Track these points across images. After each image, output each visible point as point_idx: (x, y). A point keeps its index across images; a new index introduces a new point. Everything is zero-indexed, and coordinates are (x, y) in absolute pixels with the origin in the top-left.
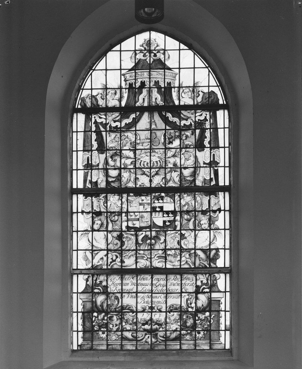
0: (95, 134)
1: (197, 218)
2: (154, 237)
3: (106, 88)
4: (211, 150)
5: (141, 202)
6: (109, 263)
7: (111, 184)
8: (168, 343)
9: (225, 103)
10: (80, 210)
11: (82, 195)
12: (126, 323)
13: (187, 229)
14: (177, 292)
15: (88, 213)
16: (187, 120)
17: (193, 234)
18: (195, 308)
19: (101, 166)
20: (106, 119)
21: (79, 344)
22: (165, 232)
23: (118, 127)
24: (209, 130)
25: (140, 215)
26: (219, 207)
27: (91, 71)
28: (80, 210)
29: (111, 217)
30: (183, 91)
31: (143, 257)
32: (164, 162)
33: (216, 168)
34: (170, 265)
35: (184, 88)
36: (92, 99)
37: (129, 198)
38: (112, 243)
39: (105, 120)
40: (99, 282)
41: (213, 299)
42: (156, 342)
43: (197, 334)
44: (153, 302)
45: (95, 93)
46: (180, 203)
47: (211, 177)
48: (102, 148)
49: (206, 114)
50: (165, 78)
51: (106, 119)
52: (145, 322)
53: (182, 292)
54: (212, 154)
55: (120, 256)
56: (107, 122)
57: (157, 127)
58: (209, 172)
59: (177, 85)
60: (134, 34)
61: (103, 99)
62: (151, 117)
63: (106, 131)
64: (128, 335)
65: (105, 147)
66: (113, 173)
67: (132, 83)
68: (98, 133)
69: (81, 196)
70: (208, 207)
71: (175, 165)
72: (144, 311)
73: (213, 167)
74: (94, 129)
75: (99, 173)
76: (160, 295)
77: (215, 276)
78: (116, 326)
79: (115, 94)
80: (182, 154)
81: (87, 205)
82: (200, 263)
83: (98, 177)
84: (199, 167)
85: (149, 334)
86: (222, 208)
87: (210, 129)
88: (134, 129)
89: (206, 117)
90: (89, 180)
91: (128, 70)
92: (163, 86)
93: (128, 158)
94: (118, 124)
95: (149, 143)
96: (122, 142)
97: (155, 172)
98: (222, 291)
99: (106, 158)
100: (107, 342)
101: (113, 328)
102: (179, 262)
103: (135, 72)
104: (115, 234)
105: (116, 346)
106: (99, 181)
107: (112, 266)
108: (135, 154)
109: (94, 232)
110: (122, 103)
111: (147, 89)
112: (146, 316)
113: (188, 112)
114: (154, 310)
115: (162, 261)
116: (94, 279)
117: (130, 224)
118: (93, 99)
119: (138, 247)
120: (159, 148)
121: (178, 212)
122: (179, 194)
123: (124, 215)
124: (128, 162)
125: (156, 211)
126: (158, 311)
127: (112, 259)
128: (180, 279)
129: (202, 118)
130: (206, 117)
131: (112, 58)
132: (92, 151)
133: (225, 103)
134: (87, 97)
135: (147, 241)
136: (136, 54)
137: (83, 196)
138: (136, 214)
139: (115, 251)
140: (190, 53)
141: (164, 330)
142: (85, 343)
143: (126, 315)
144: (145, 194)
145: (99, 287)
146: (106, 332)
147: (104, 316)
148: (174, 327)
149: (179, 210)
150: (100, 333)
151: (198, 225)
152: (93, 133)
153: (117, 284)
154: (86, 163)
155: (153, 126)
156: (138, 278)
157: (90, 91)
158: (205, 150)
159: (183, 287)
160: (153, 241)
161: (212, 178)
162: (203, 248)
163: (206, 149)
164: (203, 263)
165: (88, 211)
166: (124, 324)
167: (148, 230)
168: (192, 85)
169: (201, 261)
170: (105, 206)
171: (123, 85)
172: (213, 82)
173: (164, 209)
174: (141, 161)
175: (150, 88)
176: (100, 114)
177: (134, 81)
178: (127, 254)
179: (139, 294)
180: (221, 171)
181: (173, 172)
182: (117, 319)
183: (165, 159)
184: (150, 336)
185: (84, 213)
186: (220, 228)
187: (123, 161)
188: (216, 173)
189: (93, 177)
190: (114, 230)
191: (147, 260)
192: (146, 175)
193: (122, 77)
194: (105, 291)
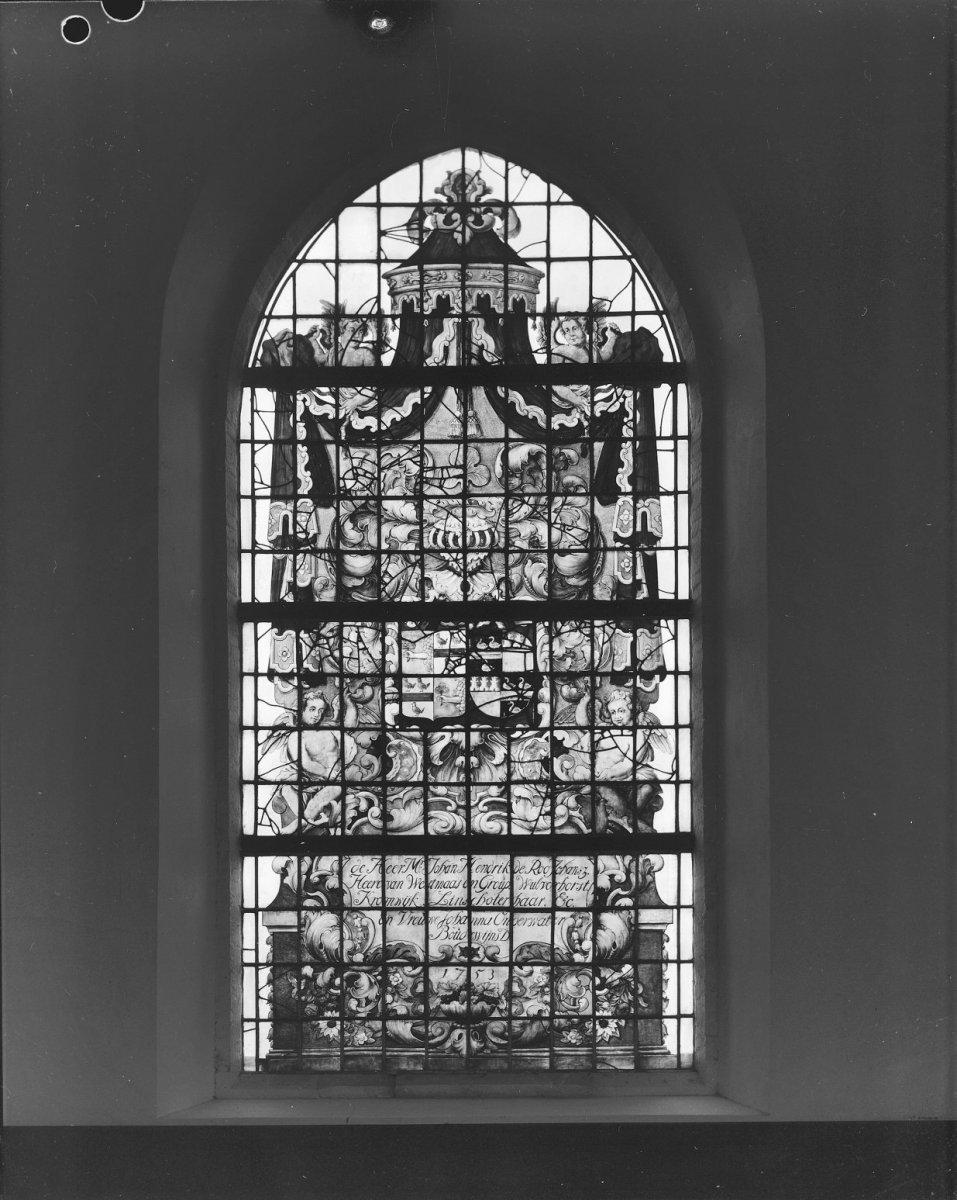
0: (305, 448)
1: (600, 694)
2: (477, 747)
3: (335, 314)
4: (635, 501)
5: (437, 646)
6: (349, 822)
7: (350, 596)
8: (518, 1052)
9: (678, 360)
10: (263, 669)
12: (396, 997)
13: (571, 725)
14: (542, 906)
15: (286, 677)
16: (568, 412)
17: (586, 739)
18: (591, 953)
19: (322, 543)
20: (337, 406)
21: (263, 1056)
22: (508, 733)
23: (373, 430)
24: (629, 443)
25: (436, 685)
26: (660, 663)
27: (294, 265)
28: (263, 669)
29: (352, 690)
30: (560, 325)
31: (444, 806)
32: (502, 535)
33: (649, 553)
34: (522, 827)
35: (562, 318)
36: (294, 346)
37: (405, 634)
38: (357, 763)
40: (317, 879)
41: (644, 928)
42: (481, 1050)
43: (598, 1027)
44: (473, 936)
45: (303, 328)
46: (551, 652)
47: (638, 577)
48: (326, 492)
49: (625, 397)
50: (506, 289)
51: (337, 406)
52: (451, 993)
53: (554, 909)
54: (639, 513)
55: (379, 800)
56: (341, 416)
57: (482, 433)
58: (631, 564)
59: (541, 306)
60: (419, 158)
61: (328, 347)
62: (466, 402)
63: (338, 442)
64: (403, 1029)
65: (333, 487)
66: (359, 564)
67: (412, 300)
68: (315, 445)
70: (629, 663)
71: (534, 541)
72: (446, 962)
74: (302, 433)
75: (316, 563)
76: (493, 914)
77: (648, 860)
78: (366, 1005)
79: (364, 330)
80: (555, 512)
81: (284, 653)
82: (609, 821)
83: (313, 572)
84: (601, 550)
85: (461, 1028)
86: (670, 667)
87: (633, 440)
88: (416, 437)
89: (622, 404)
90: (289, 583)
91: (399, 264)
92: (500, 310)
93: (399, 521)
94: (371, 422)
95: (461, 480)
97: (478, 562)
98: (670, 904)
99: (337, 520)
100: (342, 1051)
101: (359, 1010)
102: (549, 818)
103: (422, 273)
104: (365, 738)
105: (367, 1060)
106: (317, 585)
107: (358, 828)
108: (419, 509)
109: (305, 733)
111: (456, 320)
112: (453, 976)
114: (476, 959)
115: (499, 817)
116: (304, 868)
117: (408, 710)
118: (301, 346)
119: (430, 776)
120: (488, 492)
121: (545, 677)
122: (547, 624)
123: (389, 682)
124: (401, 532)
125: (482, 674)
126: (486, 960)
127: (357, 808)
128: (550, 871)
130: (622, 404)
131: (355, 228)
132: (296, 497)
133: (678, 360)
134: (281, 341)
135: (455, 758)
136: (423, 217)
138: (425, 681)
139: (365, 785)
140: (580, 215)
141: (503, 1015)
142: (280, 1053)
143: (396, 972)
144: (451, 624)
145: (318, 893)
146: (338, 1023)
147: (331, 975)
148: (533, 1006)
149: (548, 670)
150: (323, 1024)
151: (601, 714)
152: (299, 446)
153: (369, 885)
155: (472, 431)
156: (431, 867)
157: (288, 324)
158: (620, 502)
159: (558, 894)
160: (474, 760)
162: (614, 779)
163: (621, 499)
164: (615, 823)
165: (288, 671)
166: (389, 998)
167: (458, 726)
169: (611, 818)
170: (334, 658)
172: (645, 302)
173: (506, 668)
174: (438, 530)
175: (464, 315)
176: (320, 392)
177: (418, 295)
178: (401, 795)
179: (432, 914)
180: (664, 560)
181: (530, 561)
182: (371, 985)
183: (507, 525)
184: (464, 1032)
185: (276, 679)
186: (663, 723)
187: (385, 529)
190: (361, 726)
191: (455, 812)
192: (451, 569)
194: (336, 902)
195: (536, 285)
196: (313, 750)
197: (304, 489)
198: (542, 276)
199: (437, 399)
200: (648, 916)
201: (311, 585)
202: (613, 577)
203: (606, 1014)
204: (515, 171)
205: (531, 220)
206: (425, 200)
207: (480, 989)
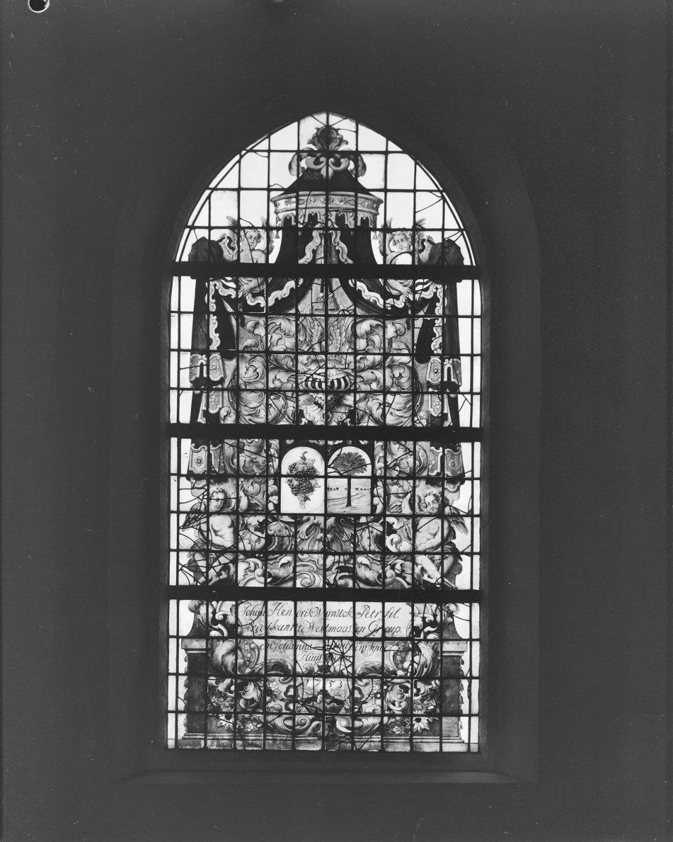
0: (215, 317)
9: (474, 264)
10: (184, 471)
11: (190, 440)
16: (397, 298)
20: (237, 290)
24: (440, 319)
27: (207, 192)
28: (184, 471)
30: (392, 238)
33: (452, 396)
39: (235, 292)
43: (414, 722)
45: (216, 235)
47: (445, 412)
48: (230, 349)
56: (239, 297)
59: (380, 224)
60: (298, 118)
61: (233, 249)
62: (327, 287)
68: (221, 313)
69: (187, 444)
72: (310, 674)
73: (447, 393)
74: (213, 307)
83: (219, 404)
86: (468, 475)
88: (293, 311)
89: (435, 293)
90: (204, 411)
92: (352, 226)
96: (269, 336)
103: (297, 197)
106: (223, 413)
110: (270, 256)
112: (312, 685)
113: (401, 283)
123: (271, 482)
129: (428, 295)
130: (435, 293)
133: (474, 264)
136: (300, 159)
137: (192, 443)
150: (222, 717)
152: (211, 316)
154: (198, 376)
161: (447, 414)
163: (433, 358)
168: (410, 226)
171: (273, 223)
172: (451, 223)
175: (326, 228)
176: (226, 281)
177: (294, 212)
188: (454, 405)
189: (211, 404)
193: (272, 205)
194: (234, 631)
195: (377, 209)
196: (216, 529)
197: (214, 347)
198: (382, 202)
199: (306, 288)
200: (449, 647)
201: (218, 413)
202: (428, 412)
203: (420, 712)
204: (363, 129)
205: (373, 164)
206: (301, 149)
207: (332, 694)
